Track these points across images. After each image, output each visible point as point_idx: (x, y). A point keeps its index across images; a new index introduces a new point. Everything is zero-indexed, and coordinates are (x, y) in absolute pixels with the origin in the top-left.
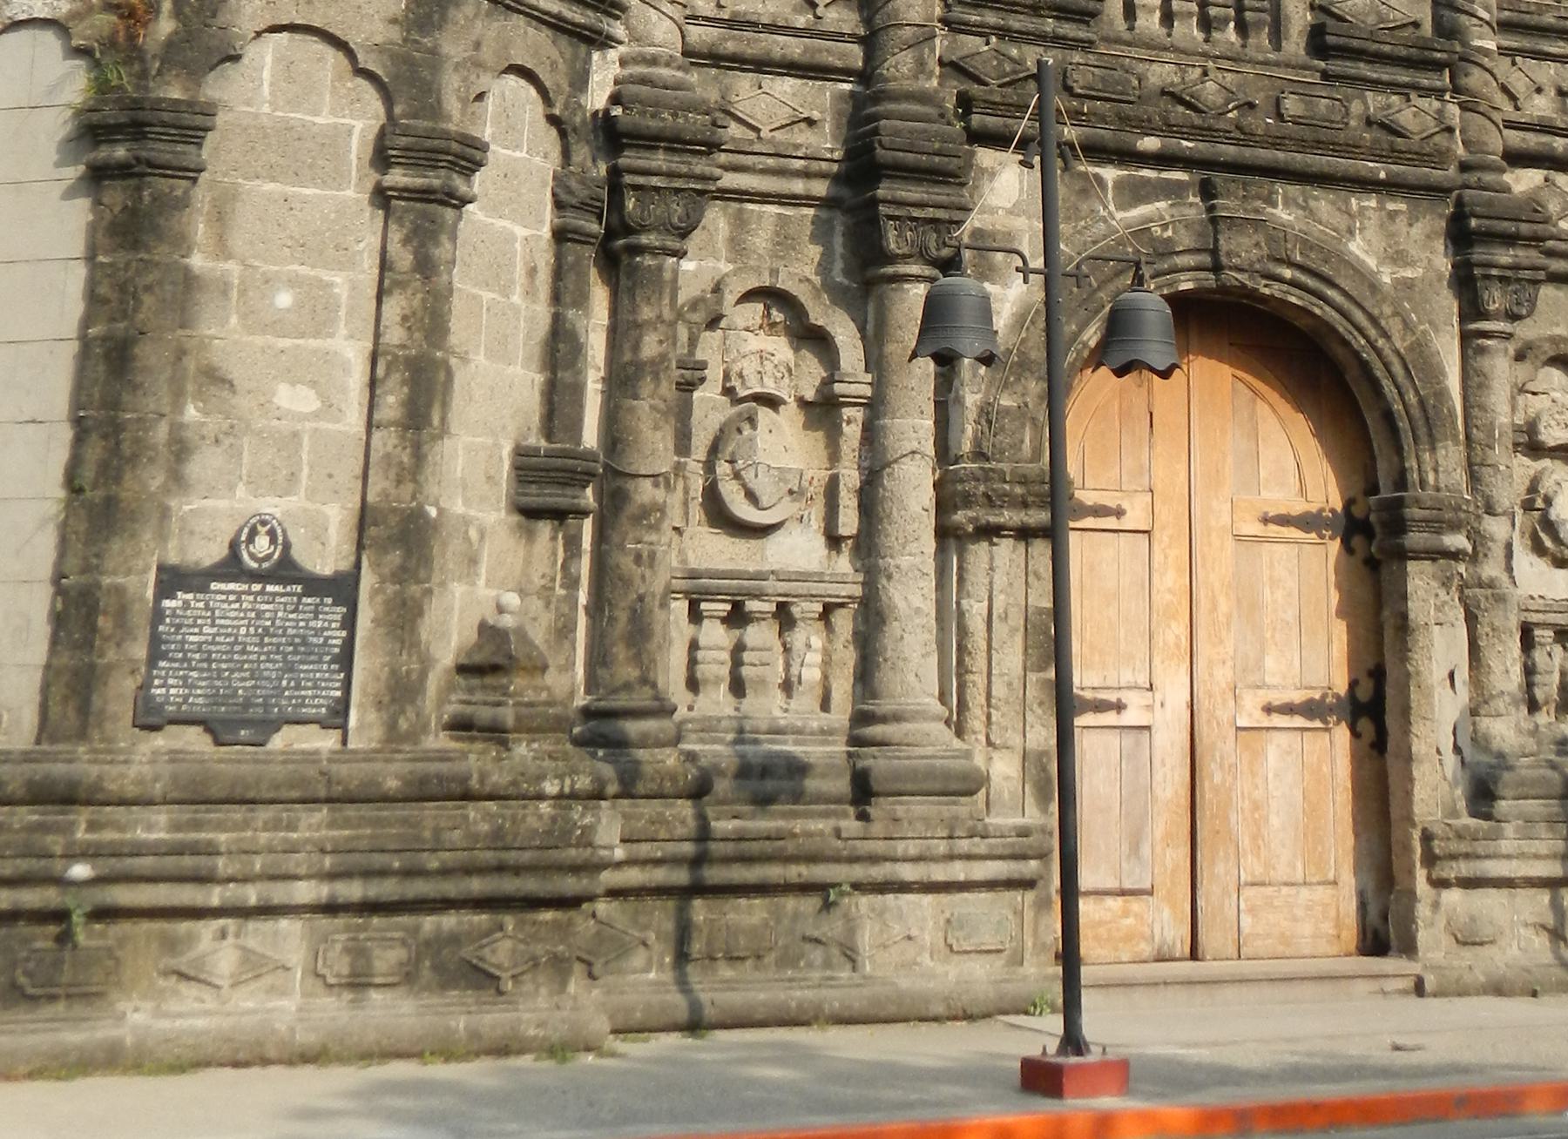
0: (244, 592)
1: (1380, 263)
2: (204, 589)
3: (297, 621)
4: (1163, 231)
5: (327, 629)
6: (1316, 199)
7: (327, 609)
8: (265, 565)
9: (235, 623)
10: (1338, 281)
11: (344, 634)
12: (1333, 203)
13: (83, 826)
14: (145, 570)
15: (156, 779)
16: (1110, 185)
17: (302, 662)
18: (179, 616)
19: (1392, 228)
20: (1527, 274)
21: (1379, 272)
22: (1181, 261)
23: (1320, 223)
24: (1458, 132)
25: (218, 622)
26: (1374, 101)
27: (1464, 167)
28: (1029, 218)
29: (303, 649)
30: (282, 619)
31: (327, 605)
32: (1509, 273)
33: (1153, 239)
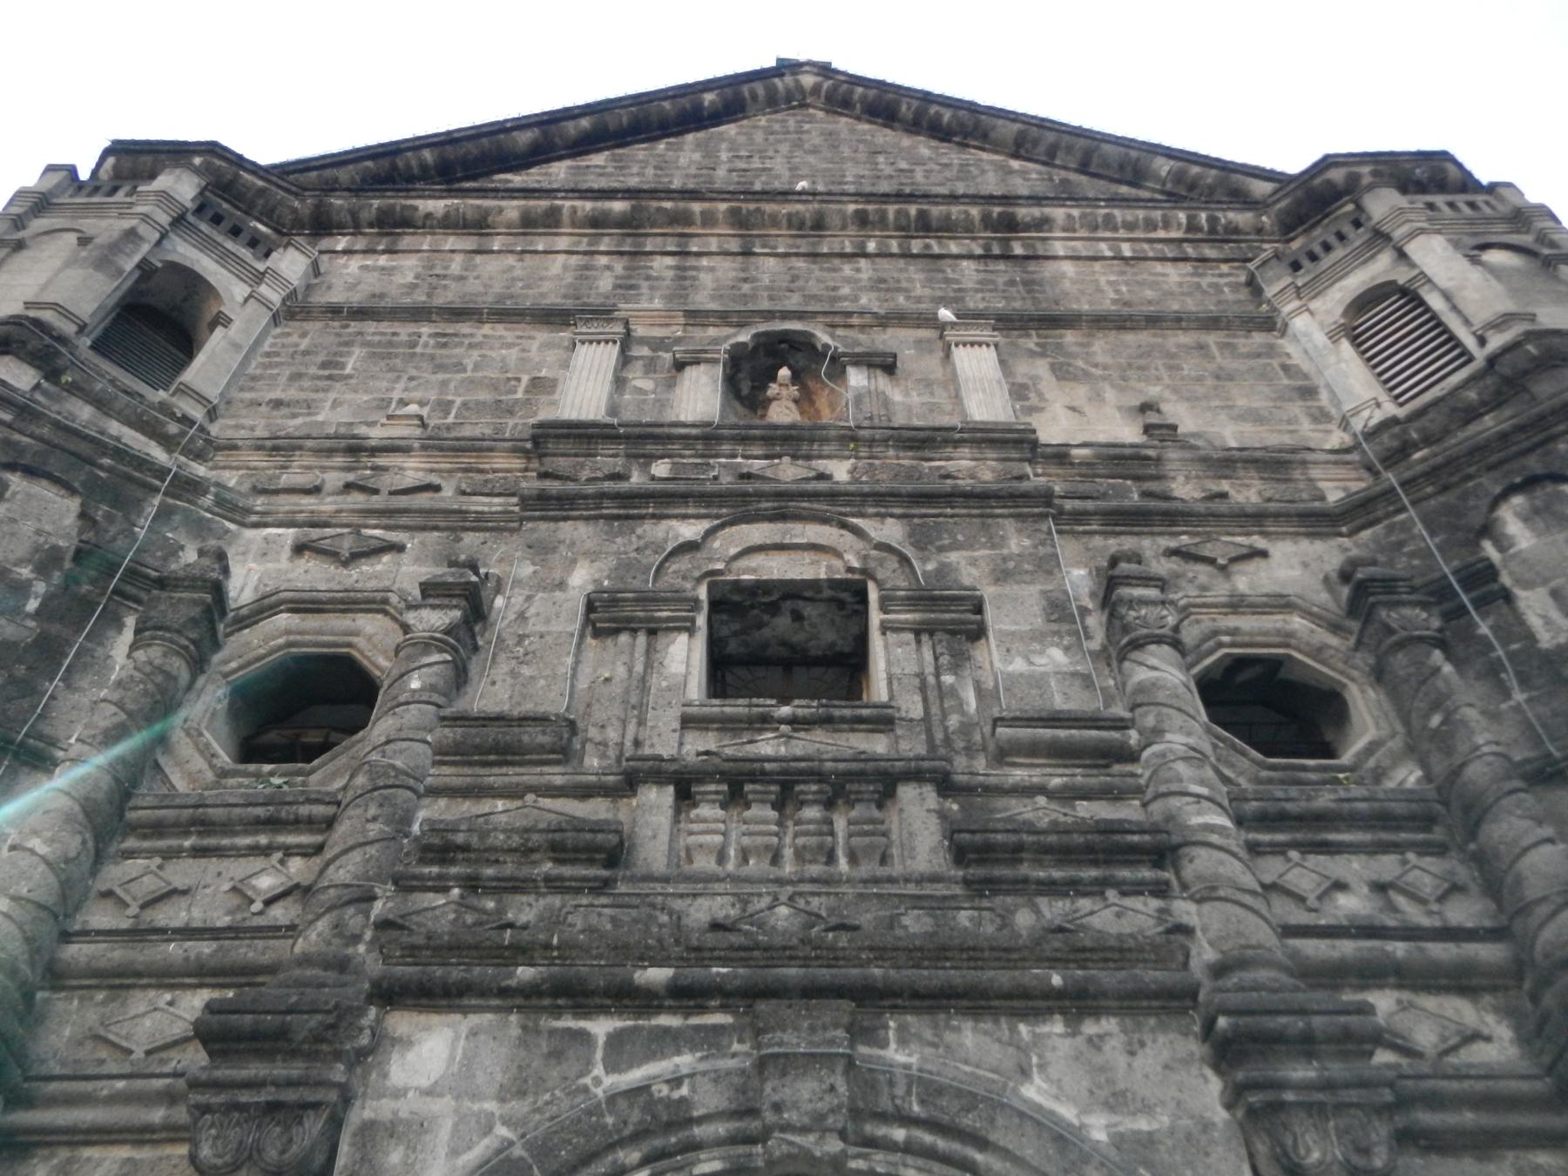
1: (1085, 1111)
4: (672, 1090)
6: (958, 1030)
10: (993, 1137)
12: (986, 1033)
16: (601, 1041)
19: (1098, 1059)
20: (1353, 1095)
21: (1082, 1126)
22: (698, 1131)
23: (966, 1062)
24: (1199, 933)
26: (1054, 909)
27: (1219, 970)
28: (457, 1098)
32: (1319, 1096)
33: (651, 1105)
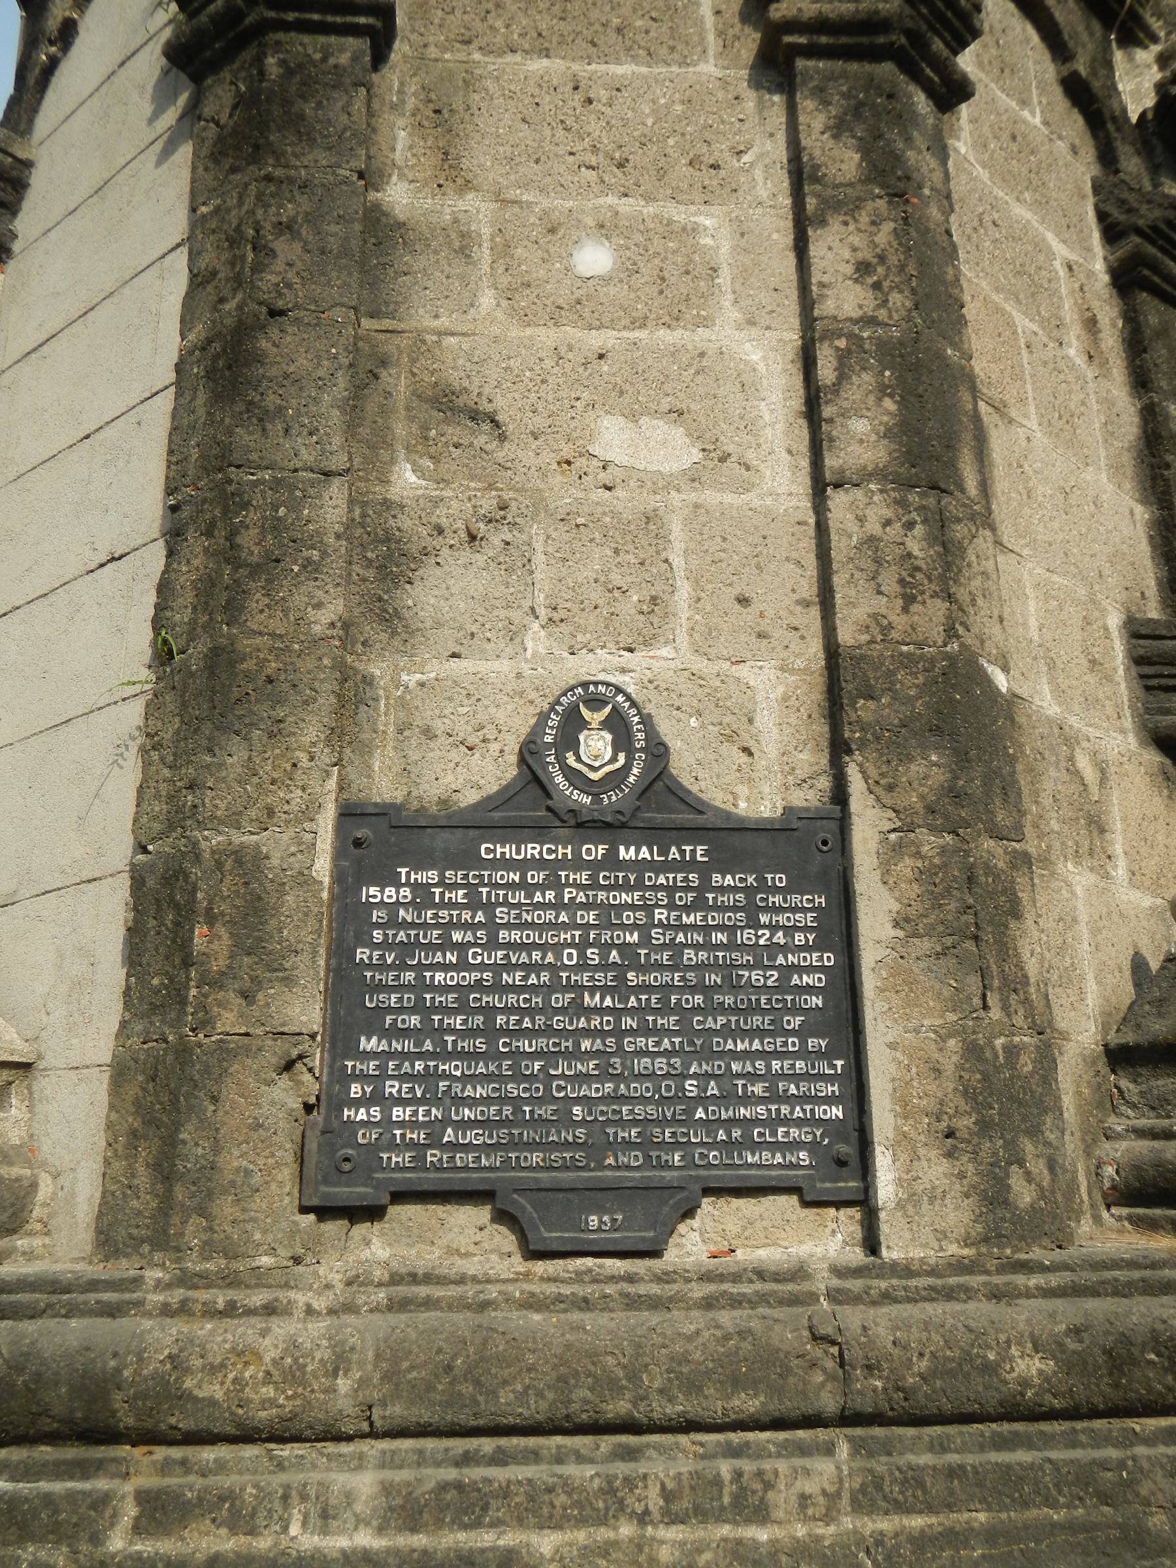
0: (562, 863)
2: (468, 859)
3: (706, 929)
5: (784, 949)
7: (777, 899)
8: (611, 798)
9: (549, 937)
11: (829, 959)
13: (130, 1511)
14: (309, 812)
15: (339, 1364)
17: (728, 1032)
18: (405, 925)
25: (503, 934)
29: (729, 1000)
30: (667, 927)
31: (776, 890)
